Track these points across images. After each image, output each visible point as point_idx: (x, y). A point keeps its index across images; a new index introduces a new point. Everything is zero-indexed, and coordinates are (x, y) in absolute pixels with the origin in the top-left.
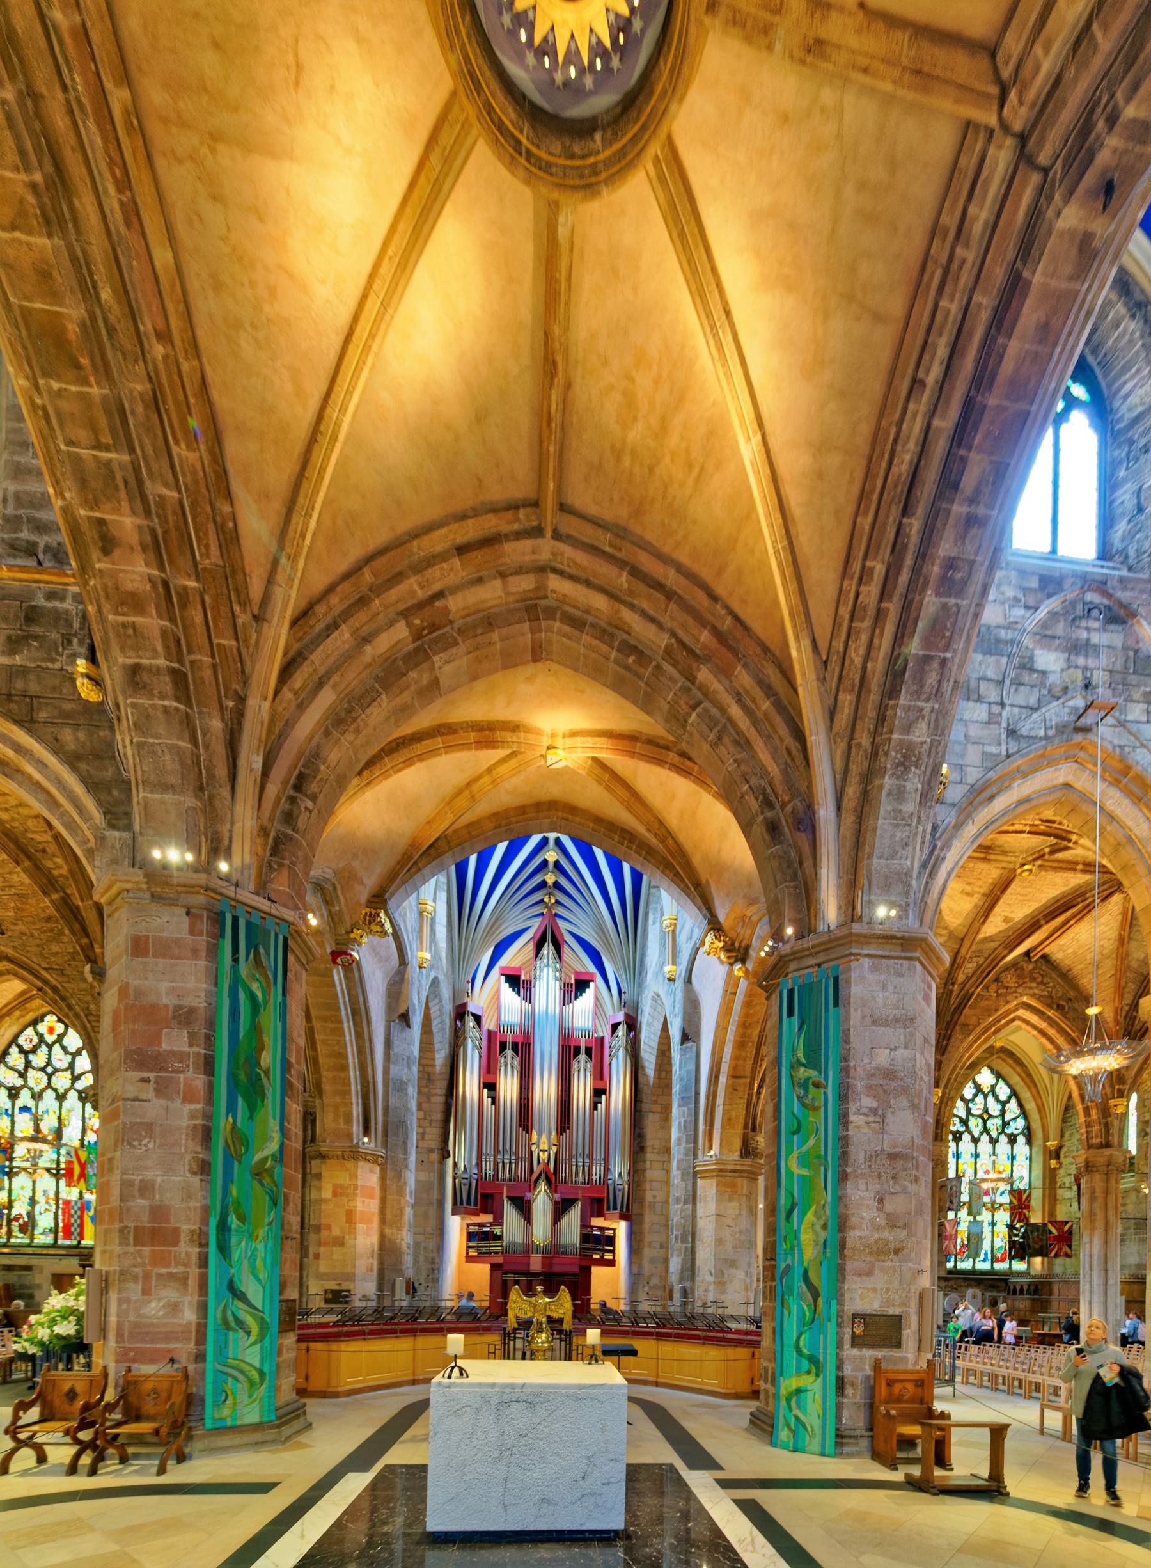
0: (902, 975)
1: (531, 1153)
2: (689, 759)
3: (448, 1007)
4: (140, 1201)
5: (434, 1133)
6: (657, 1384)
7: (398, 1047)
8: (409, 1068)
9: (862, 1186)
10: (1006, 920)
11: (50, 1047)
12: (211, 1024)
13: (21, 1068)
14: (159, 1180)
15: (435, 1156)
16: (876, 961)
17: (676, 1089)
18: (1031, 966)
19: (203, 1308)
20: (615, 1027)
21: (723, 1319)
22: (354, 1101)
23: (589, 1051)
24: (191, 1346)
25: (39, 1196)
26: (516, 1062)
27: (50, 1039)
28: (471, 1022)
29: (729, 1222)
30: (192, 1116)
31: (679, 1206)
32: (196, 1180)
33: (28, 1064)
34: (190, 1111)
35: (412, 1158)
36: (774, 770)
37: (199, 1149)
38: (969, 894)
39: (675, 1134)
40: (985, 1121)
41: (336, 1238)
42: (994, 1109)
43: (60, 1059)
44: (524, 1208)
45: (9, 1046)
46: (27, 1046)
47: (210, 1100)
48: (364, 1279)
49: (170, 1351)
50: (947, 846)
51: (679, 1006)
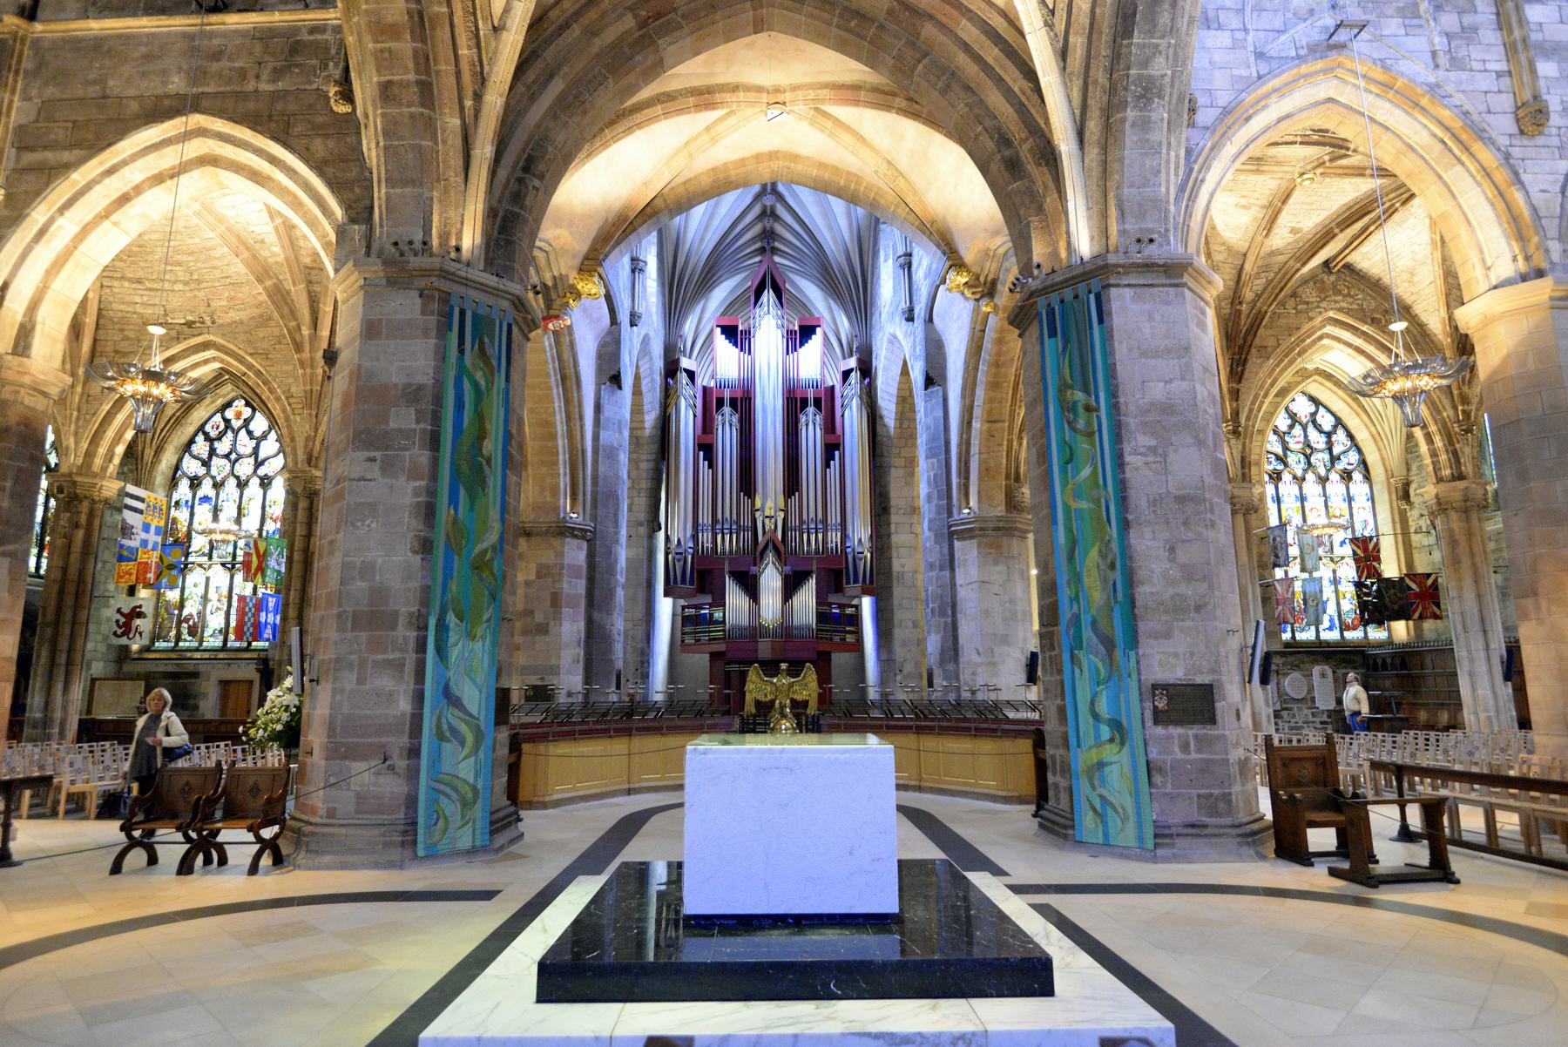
0: (1169, 303)
3: (659, 363)
4: (360, 583)
5: (642, 502)
6: (919, 789)
9: (1148, 535)
10: (1293, 231)
11: (236, 432)
12: (438, 400)
13: (205, 456)
14: (380, 560)
15: (643, 530)
16: (1139, 290)
17: (922, 439)
18: (1333, 278)
19: (419, 697)
20: (846, 375)
21: (996, 706)
22: (561, 471)
23: (817, 403)
24: (404, 740)
25: (212, 595)
26: (735, 419)
27: (236, 424)
28: (683, 378)
29: (995, 589)
30: (416, 493)
31: (934, 574)
32: (416, 560)
33: (212, 452)
34: (415, 488)
35: (624, 532)
37: (421, 527)
38: (1244, 207)
40: (1308, 458)
41: (540, 625)
42: (1318, 440)
43: (245, 444)
44: (751, 587)
45: (196, 434)
46: (213, 434)
47: (434, 476)
48: (569, 673)
49: (383, 746)
50: (1206, 167)
51: (920, 350)
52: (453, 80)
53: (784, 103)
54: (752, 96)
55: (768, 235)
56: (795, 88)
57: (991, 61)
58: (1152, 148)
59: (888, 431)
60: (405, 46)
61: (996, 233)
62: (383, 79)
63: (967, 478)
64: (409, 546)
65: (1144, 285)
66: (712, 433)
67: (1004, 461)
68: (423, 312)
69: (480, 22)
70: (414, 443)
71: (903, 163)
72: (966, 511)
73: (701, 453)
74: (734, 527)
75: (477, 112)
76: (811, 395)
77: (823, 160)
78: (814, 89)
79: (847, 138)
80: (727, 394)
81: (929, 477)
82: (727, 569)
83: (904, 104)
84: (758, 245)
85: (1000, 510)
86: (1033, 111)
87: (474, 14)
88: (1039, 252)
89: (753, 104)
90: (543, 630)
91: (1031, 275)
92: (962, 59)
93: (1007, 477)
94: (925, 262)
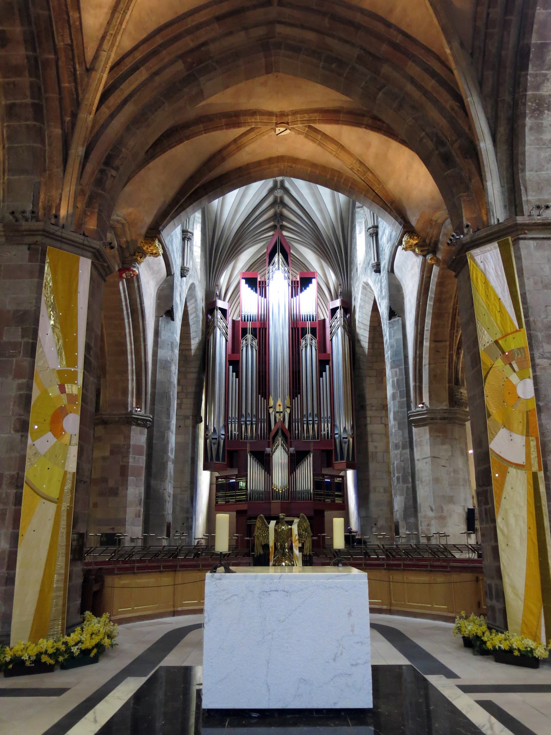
1: (269, 415)
2: (380, 120)
3: (201, 304)
6: (389, 612)
7: (164, 335)
8: (172, 351)
15: (189, 422)
17: (388, 354)
20: (334, 311)
21: (446, 549)
23: (313, 331)
26: (255, 343)
28: (219, 314)
29: (443, 462)
31: (398, 451)
36: (443, 122)
39: (390, 391)
48: (133, 524)
51: (385, 292)
52: (57, 103)
53: (288, 123)
54: (265, 119)
55: (279, 217)
56: (295, 113)
57: (429, 88)
58: (544, 144)
59: (364, 351)
60: (25, 80)
61: (438, 209)
62: (9, 102)
63: (421, 381)
64: (12, 426)
65: (543, 239)
66: (238, 353)
67: (447, 369)
68: (30, 260)
69: (77, 66)
70: (20, 352)
71: (371, 162)
72: (420, 405)
73: (231, 367)
74: (254, 420)
75: (73, 124)
76: (308, 325)
77: (315, 162)
78: (308, 113)
79: (332, 147)
80: (249, 325)
81: (393, 382)
82: (248, 449)
83: (370, 122)
84: (272, 224)
85: (444, 406)
86: (460, 122)
87: (73, 59)
88: (466, 217)
89: (266, 124)
90: (114, 492)
91: (463, 233)
92: (409, 87)
93: (450, 382)
94: (387, 232)
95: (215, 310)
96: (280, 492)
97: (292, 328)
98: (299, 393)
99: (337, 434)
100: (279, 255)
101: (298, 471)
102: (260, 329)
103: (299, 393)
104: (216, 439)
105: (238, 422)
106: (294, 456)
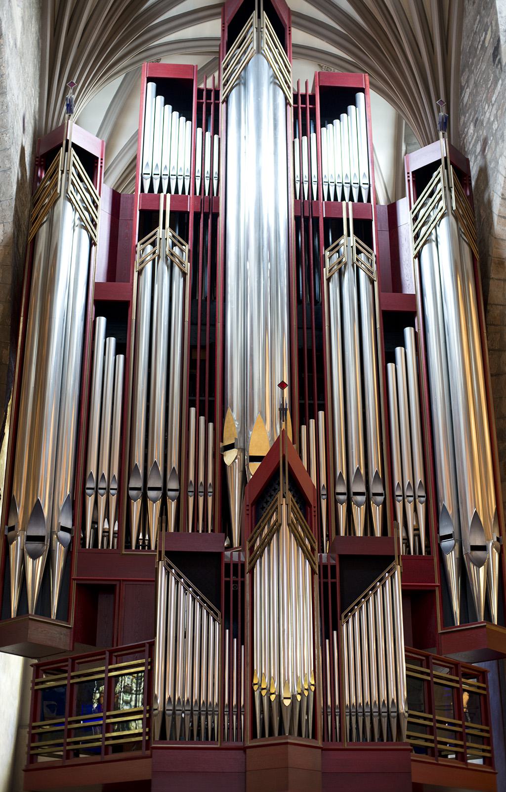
23: (363, 229)
26: (183, 253)
66: (128, 279)
73: (102, 321)
74: (173, 484)
76: (347, 213)
80: (165, 205)
95: (62, 150)
96: (287, 703)
97: (297, 219)
98: (323, 407)
99: (449, 537)
100: (259, 17)
101: (349, 629)
102: (197, 215)
103: (323, 407)
104: (41, 539)
105: (120, 490)
106: (334, 576)
